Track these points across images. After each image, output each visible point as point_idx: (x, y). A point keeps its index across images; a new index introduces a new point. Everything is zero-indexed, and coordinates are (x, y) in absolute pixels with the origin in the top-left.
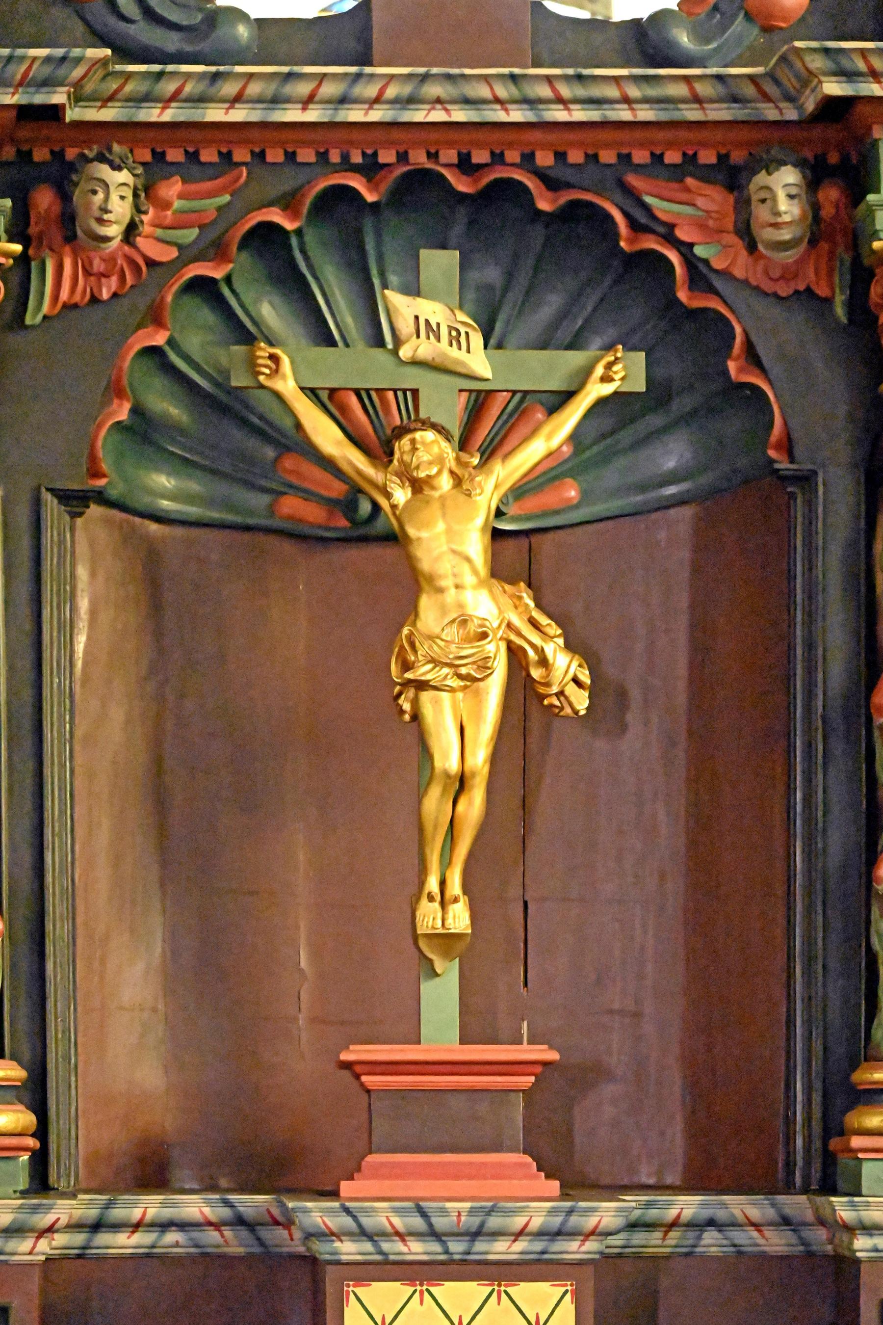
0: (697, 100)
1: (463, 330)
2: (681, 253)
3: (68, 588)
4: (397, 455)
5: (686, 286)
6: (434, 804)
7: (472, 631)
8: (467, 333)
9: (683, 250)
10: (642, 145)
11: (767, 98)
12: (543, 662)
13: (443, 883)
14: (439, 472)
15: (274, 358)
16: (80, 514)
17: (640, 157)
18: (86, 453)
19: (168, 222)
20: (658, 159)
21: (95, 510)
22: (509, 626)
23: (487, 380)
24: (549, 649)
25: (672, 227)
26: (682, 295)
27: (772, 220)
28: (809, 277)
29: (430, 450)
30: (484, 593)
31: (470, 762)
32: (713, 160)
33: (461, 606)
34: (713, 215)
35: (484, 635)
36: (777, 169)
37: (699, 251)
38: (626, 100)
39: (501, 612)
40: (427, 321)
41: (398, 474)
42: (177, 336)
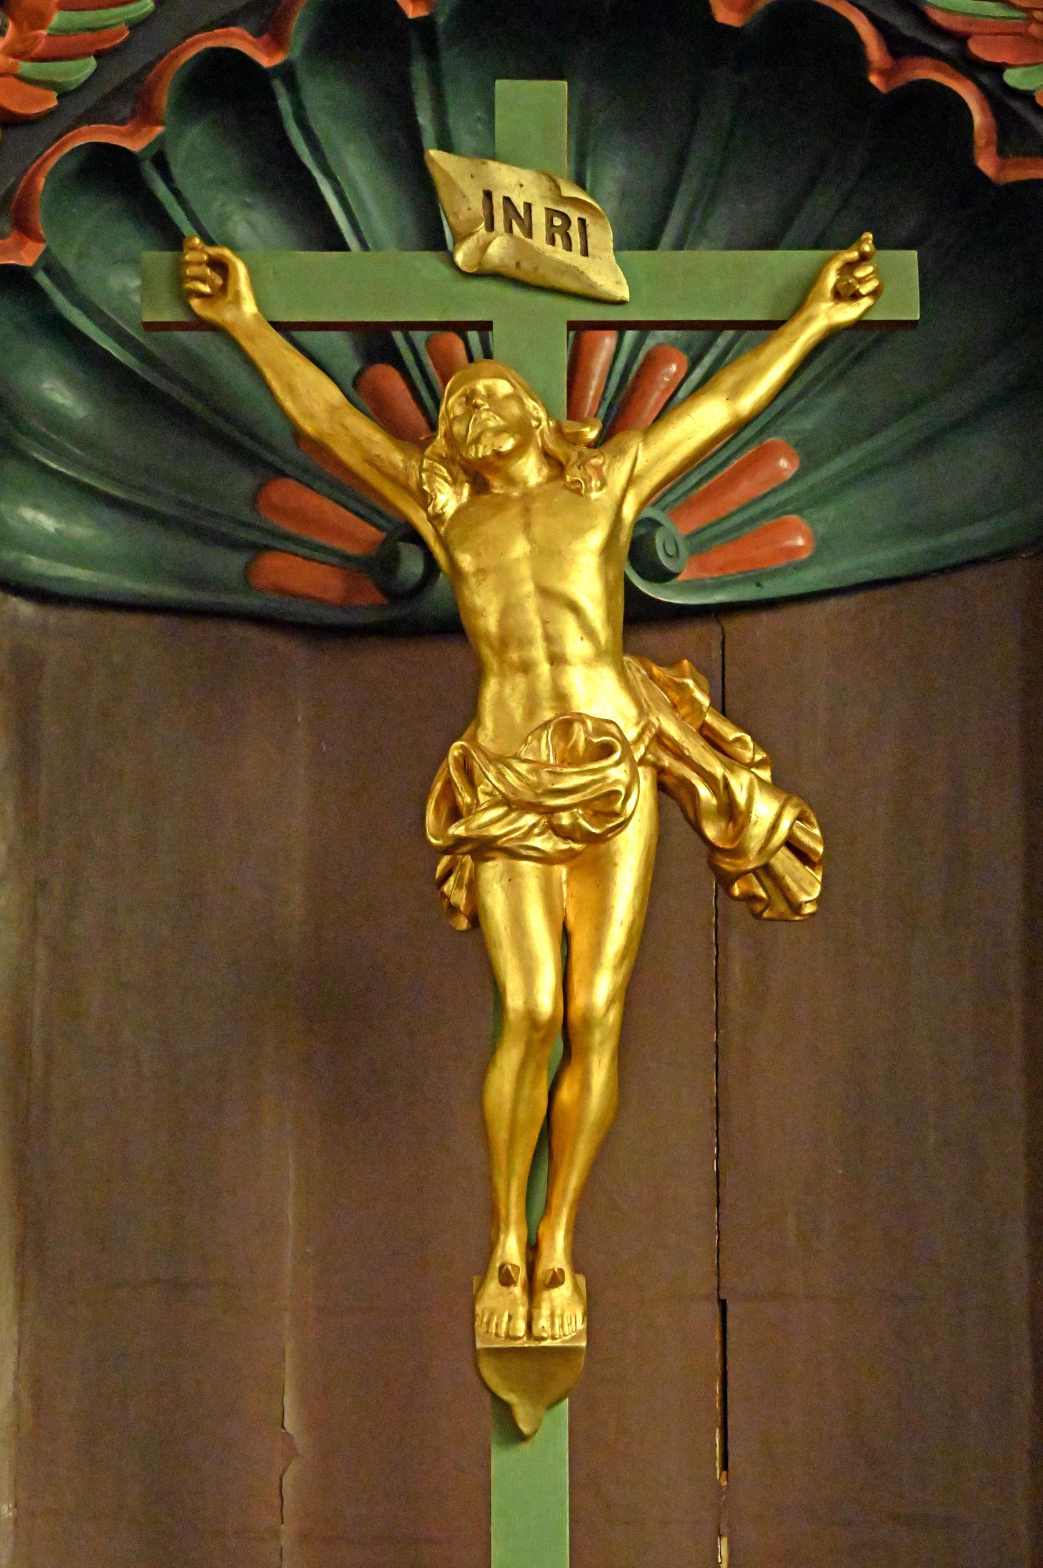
1: (574, 215)
2: (981, 86)
4: (442, 428)
6: (507, 1080)
7: (582, 744)
8: (582, 222)
9: (985, 79)
12: (732, 813)
13: (532, 1249)
14: (519, 450)
15: (220, 266)
19: (39, 49)
22: (660, 738)
23: (622, 303)
24: (740, 784)
25: (961, 39)
26: (986, 163)
29: (499, 401)
30: (607, 676)
31: (578, 1002)
33: (561, 697)
35: (607, 750)
37: (1013, 78)
39: (642, 712)
40: (507, 200)
41: (447, 461)
42: (55, 251)
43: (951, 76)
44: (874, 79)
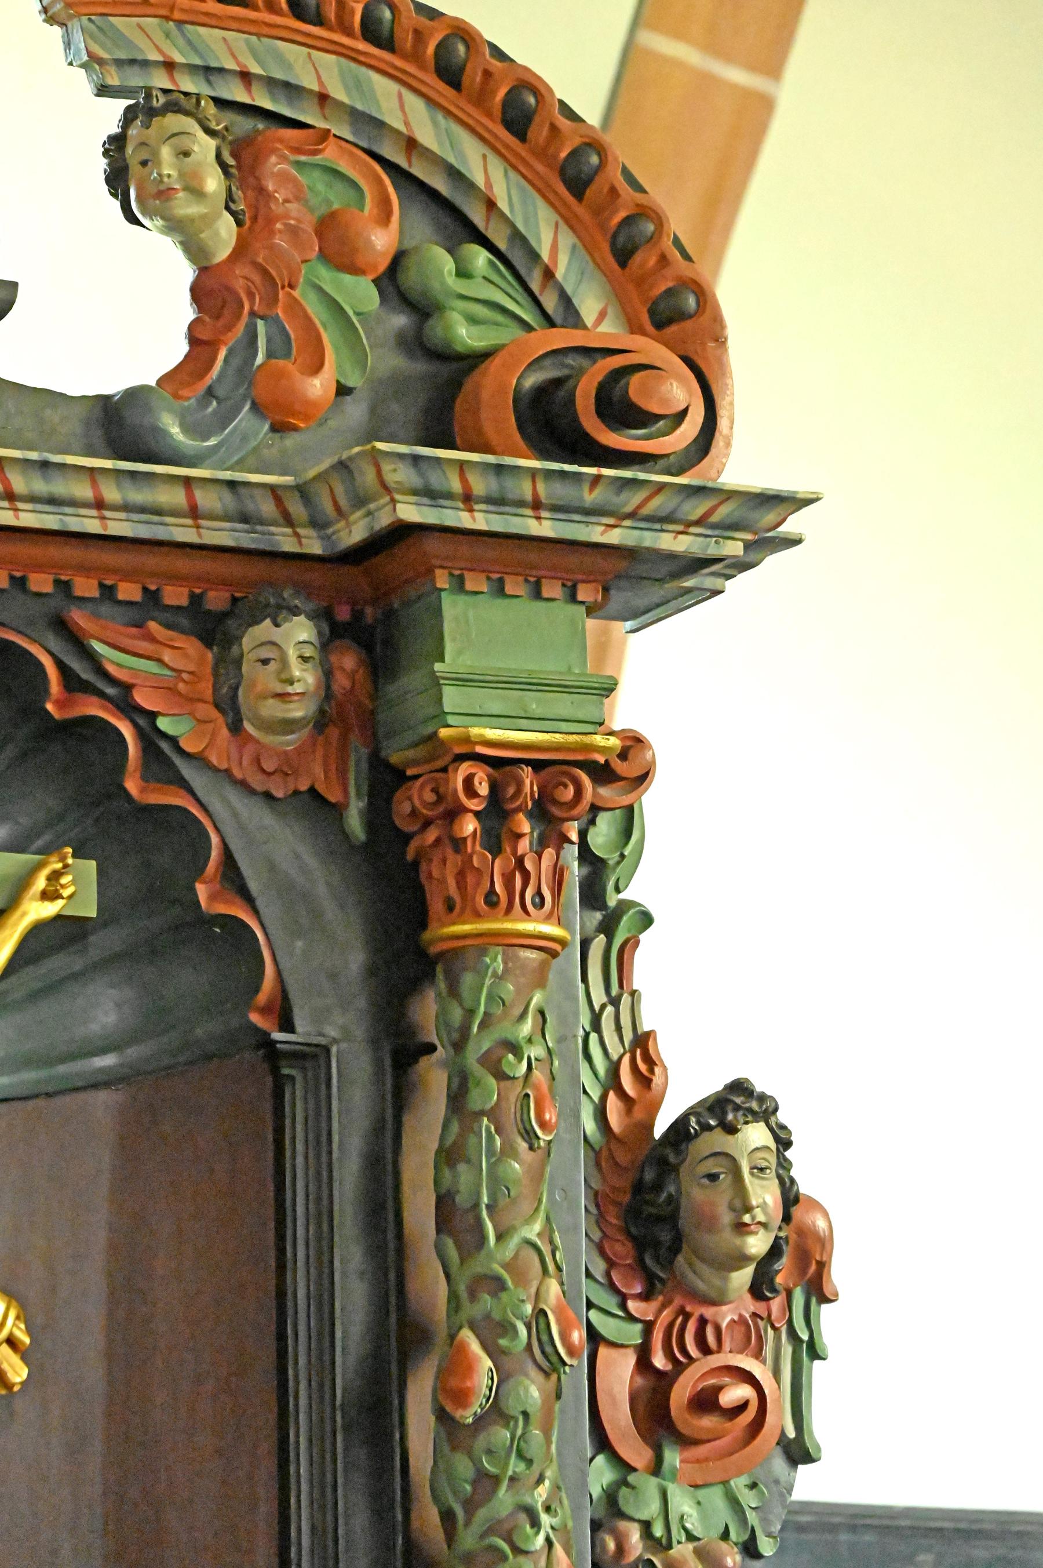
0: (194, 512)
5: (138, 774)
10: (85, 570)
11: (288, 520)
17: (86, 587)
20: (108, 592)
25: (127, 688)
26: (132, 785)
27: (279, 688)
28: (316, 774)
32: (184, 602)
34: (185, 676)
36: (285, 620)
37: (162, 723)
38: (100, 504)
43: (114, 715)
44: (49, 707)
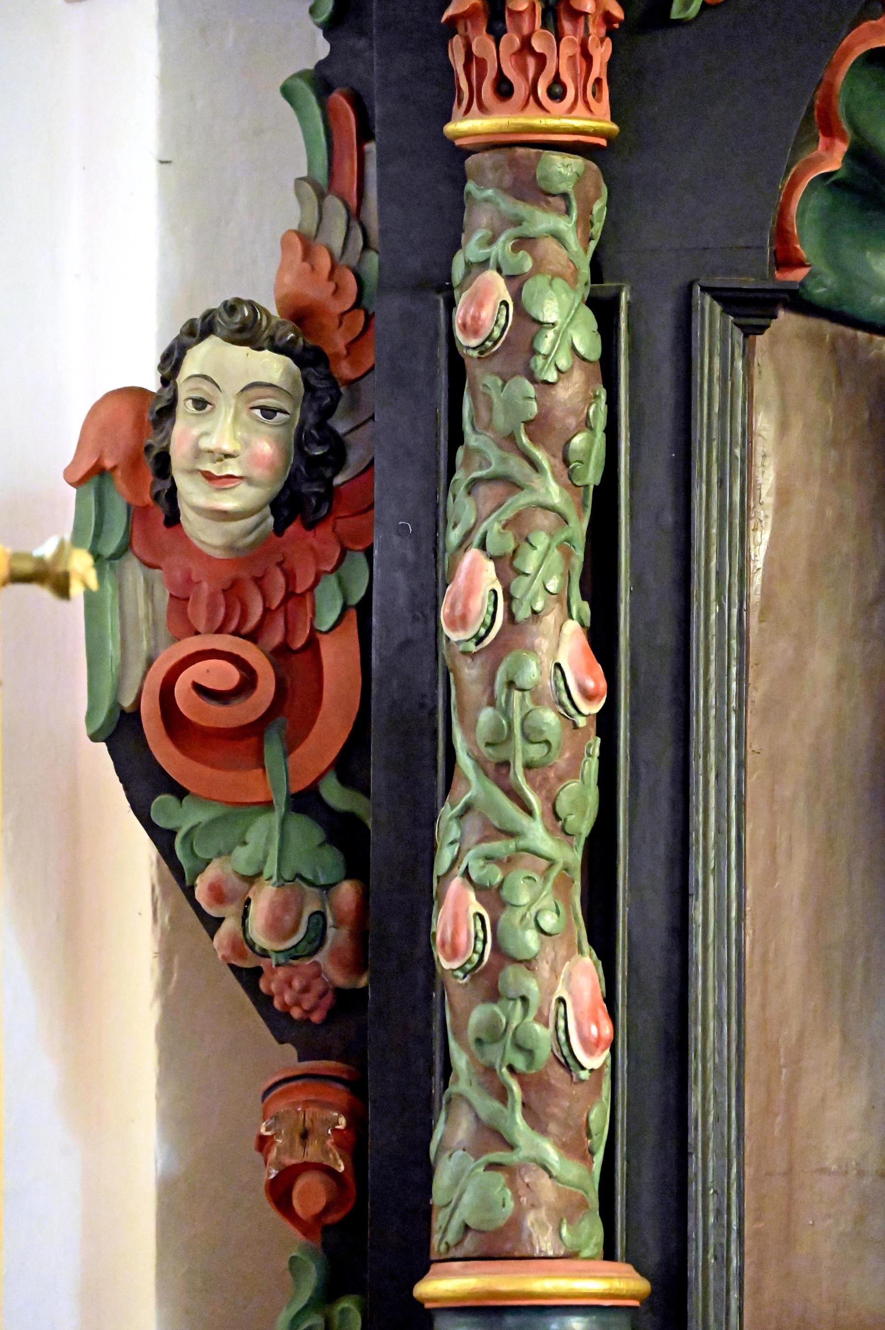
3: (738, 452)
16: (761, 329)
18: (771, 225)
21: (786, 322)
